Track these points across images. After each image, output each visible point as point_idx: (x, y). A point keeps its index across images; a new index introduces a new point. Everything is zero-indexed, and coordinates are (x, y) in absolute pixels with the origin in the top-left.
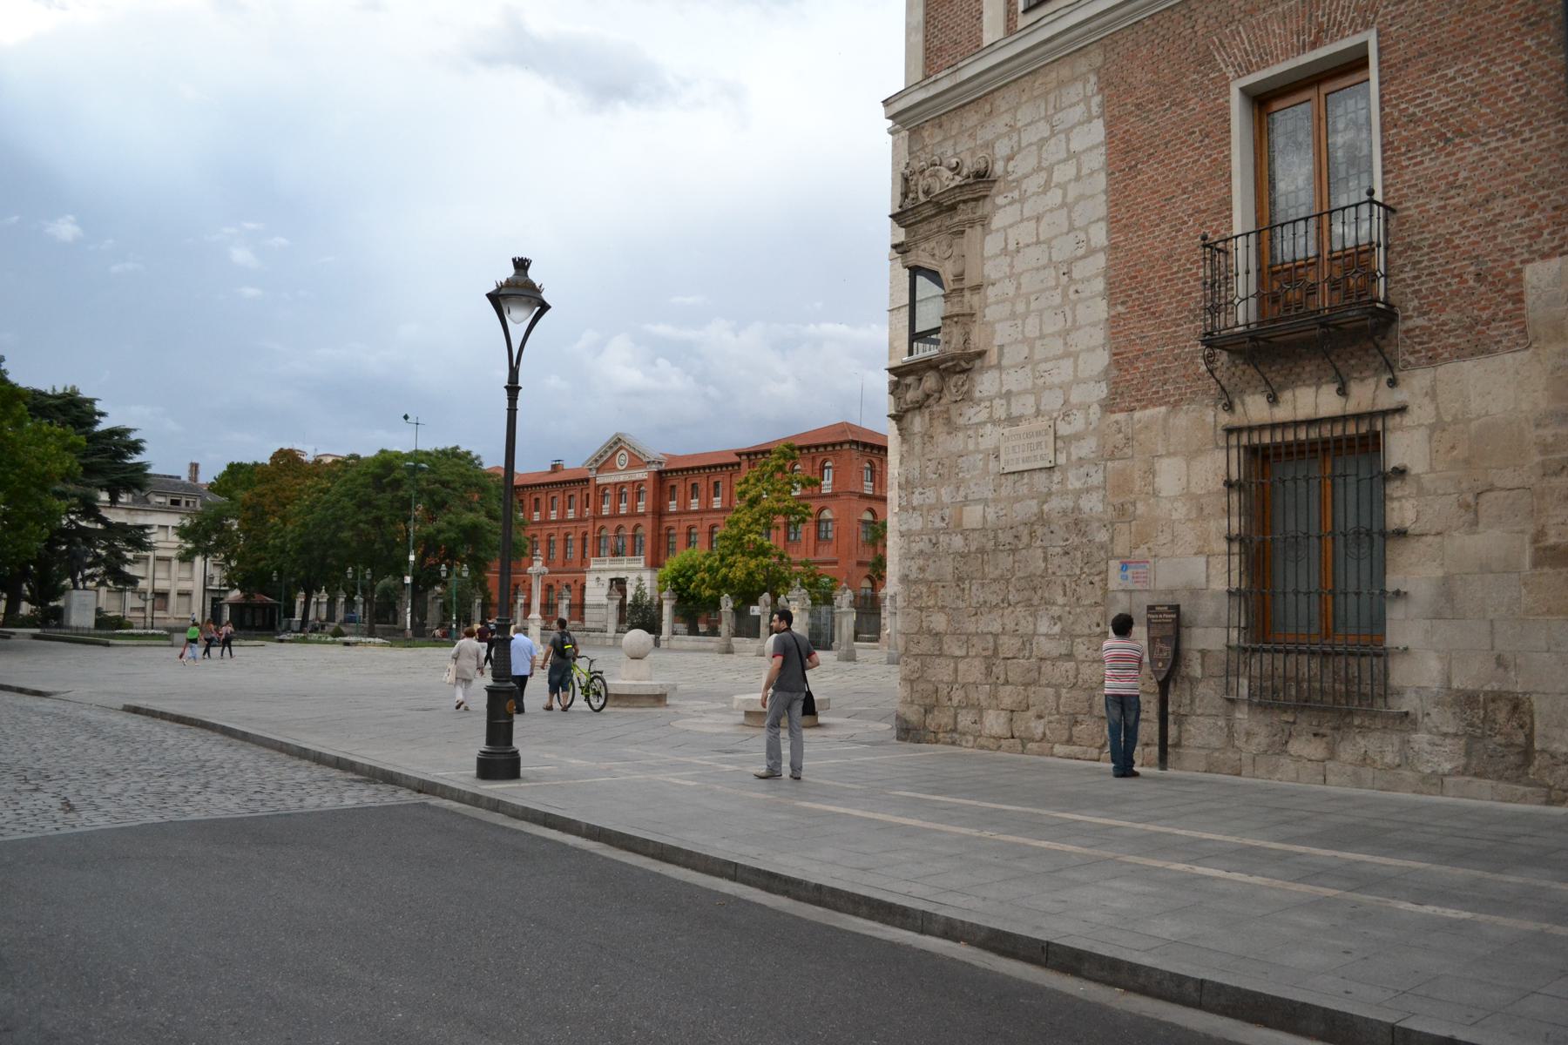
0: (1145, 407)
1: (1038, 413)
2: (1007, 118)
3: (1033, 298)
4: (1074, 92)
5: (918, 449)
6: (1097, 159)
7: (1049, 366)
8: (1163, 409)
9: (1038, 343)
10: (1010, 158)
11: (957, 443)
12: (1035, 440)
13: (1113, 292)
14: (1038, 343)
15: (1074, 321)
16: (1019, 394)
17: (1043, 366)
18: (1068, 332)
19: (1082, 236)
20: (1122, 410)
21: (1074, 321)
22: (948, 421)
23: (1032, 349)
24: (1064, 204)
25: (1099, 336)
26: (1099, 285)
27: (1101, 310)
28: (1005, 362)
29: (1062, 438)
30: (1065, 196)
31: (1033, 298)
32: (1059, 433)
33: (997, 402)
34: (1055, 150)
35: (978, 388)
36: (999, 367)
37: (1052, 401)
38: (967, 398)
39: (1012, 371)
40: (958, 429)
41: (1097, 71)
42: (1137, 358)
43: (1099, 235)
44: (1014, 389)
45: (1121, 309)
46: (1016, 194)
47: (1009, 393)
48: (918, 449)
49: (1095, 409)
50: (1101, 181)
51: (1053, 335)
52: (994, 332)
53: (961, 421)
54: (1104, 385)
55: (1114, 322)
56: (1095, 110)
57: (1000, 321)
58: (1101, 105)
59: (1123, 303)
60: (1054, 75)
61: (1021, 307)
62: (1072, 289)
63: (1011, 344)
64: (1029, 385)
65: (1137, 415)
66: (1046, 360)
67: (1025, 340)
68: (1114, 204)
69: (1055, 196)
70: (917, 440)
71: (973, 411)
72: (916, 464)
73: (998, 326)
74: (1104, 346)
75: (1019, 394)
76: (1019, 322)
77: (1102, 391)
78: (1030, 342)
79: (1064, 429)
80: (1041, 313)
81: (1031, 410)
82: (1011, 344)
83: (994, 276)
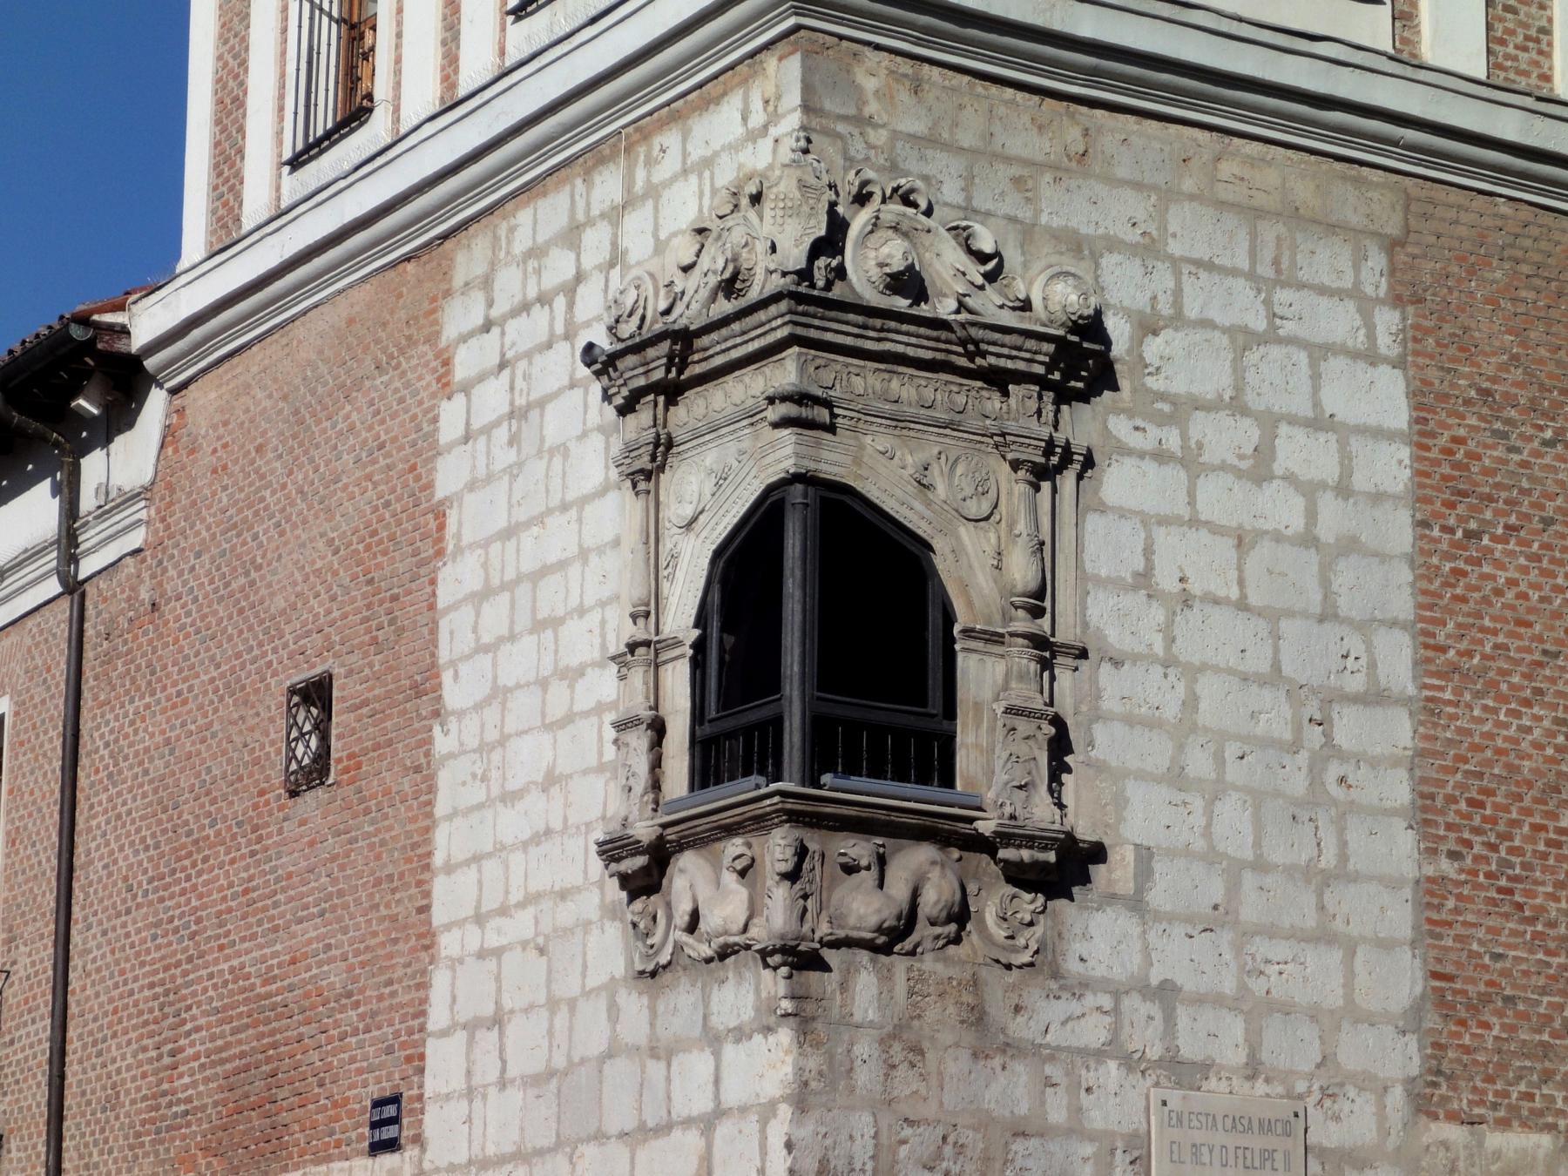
0: (1504, 1124)
1: (1253, 1070)
2: (1137, 206)
3: (1232, 750)
4: (1326, 261)
5: (867, 1077)
6: (1391, 467)
7: (1281, 950)
8: (1546, 1140)
9: (1249, 880)
10: (1148, 327)
11: (1010, 1090)
12: (1257, 1142)
13: (1424, 811)
14: (1249, 880)
15: (1343, 857)
16: (1199, 1000)
17: (1262, 947)
18: (1326, 880)
19: (1355, 644)
20: (1453, 1117)
21: (1343, 857)
22: (977, 1017)
23: (1233, 888)
24: (1308, 540)
25: (1400, 917)
26: (1399, 790)
27: (1399, 849)
28: (1157, 897)
29: (1323, 1153)
30: (1311, 515)
31: (1232, 750)
32: (1313, 1139)
33: (1134, 1005)
34: (1278, 379)
35: (1078, 948)
36: (1136, 904)
37: (1292, 1048)
38: (1043, 964)
39: (1179, 930)
40: (1011, 1048)
41: (1393, 246)
42: (1486, 999)
43: (1397, 660)
44: (1186, 981)
45: (1447, 867)
46: (1172, 439)
47: (1166, 993)
48: (867, 1077)
49: (1397, 1096)
50: (1399, 530)
51: (1290, 870)
52: (1121, 802)
53: (1022, 1029)
54: (1412, 1041)
55: (1431, 891)
56: (1386, 344)
57: (1142, 776)
58: (1402, 335)
59: (1454, 855)
60: (1271, 177)
61: (1199, 763)
62: (1334, 770)
63: (1172, 853)
64: (1229, 986)
65: (1495, 1140)
66: (1271, 932)
67: (1211, 857)
68: (1427, 601)
69: (1281, 509)
70: (864, 1048)
71: (1055, 1011)
72: (863, 1123)
73: (1135, 792)
74: (1413, 944)
75: (1199, 1000)
76: (1198, 804)
77: (1401, 1058)
78: (1234, 871)
79: (1325, 1134)
80: (1257, 798)
81: (1236, 1057)
82: (1172, 853)
83: (1116, 637)
